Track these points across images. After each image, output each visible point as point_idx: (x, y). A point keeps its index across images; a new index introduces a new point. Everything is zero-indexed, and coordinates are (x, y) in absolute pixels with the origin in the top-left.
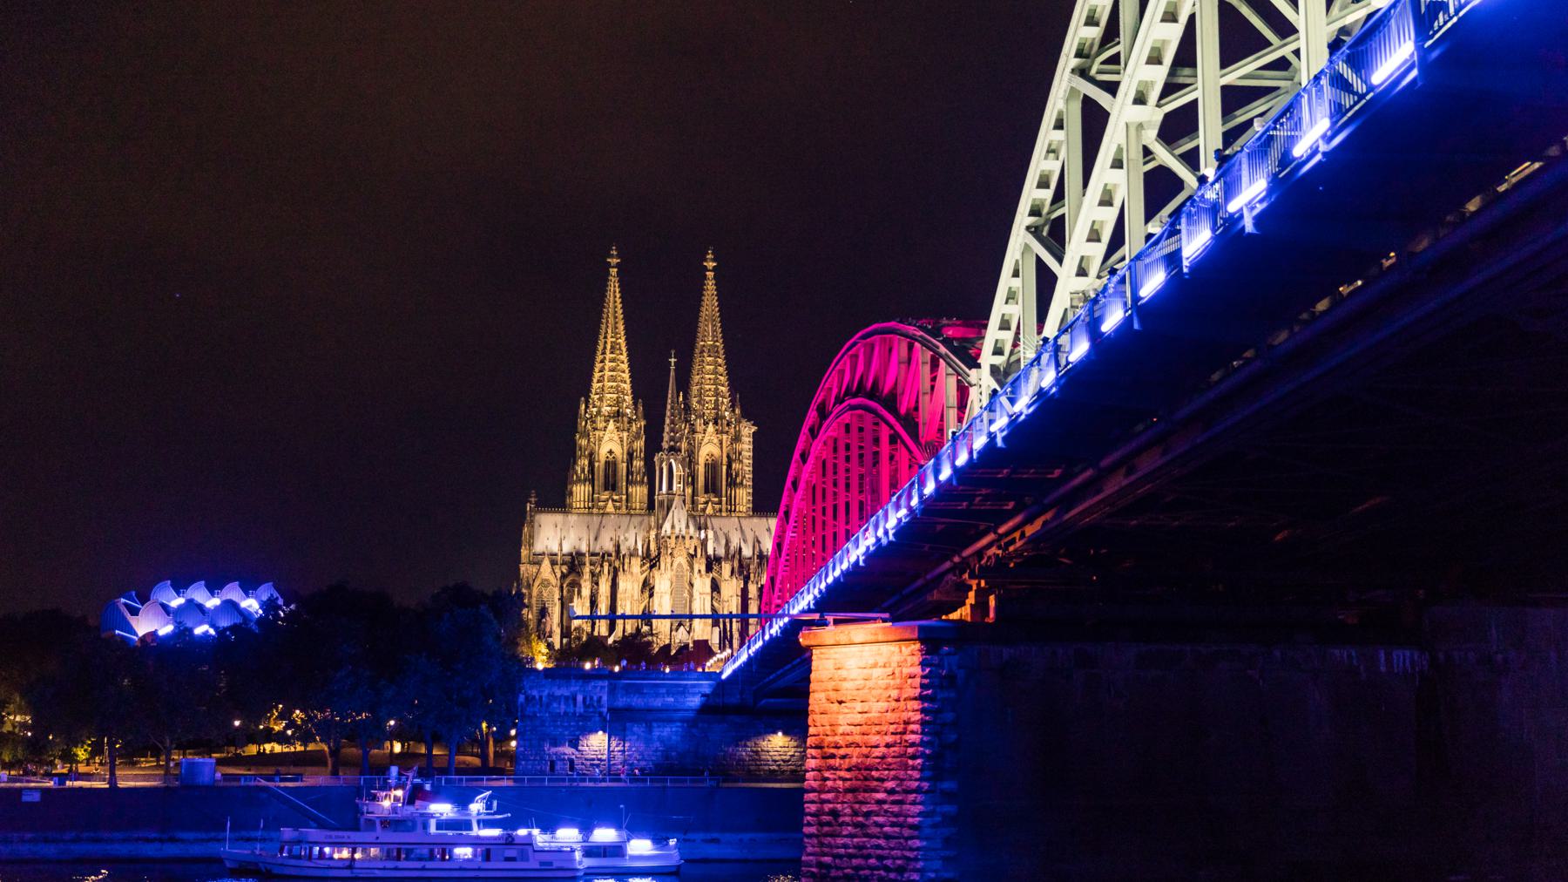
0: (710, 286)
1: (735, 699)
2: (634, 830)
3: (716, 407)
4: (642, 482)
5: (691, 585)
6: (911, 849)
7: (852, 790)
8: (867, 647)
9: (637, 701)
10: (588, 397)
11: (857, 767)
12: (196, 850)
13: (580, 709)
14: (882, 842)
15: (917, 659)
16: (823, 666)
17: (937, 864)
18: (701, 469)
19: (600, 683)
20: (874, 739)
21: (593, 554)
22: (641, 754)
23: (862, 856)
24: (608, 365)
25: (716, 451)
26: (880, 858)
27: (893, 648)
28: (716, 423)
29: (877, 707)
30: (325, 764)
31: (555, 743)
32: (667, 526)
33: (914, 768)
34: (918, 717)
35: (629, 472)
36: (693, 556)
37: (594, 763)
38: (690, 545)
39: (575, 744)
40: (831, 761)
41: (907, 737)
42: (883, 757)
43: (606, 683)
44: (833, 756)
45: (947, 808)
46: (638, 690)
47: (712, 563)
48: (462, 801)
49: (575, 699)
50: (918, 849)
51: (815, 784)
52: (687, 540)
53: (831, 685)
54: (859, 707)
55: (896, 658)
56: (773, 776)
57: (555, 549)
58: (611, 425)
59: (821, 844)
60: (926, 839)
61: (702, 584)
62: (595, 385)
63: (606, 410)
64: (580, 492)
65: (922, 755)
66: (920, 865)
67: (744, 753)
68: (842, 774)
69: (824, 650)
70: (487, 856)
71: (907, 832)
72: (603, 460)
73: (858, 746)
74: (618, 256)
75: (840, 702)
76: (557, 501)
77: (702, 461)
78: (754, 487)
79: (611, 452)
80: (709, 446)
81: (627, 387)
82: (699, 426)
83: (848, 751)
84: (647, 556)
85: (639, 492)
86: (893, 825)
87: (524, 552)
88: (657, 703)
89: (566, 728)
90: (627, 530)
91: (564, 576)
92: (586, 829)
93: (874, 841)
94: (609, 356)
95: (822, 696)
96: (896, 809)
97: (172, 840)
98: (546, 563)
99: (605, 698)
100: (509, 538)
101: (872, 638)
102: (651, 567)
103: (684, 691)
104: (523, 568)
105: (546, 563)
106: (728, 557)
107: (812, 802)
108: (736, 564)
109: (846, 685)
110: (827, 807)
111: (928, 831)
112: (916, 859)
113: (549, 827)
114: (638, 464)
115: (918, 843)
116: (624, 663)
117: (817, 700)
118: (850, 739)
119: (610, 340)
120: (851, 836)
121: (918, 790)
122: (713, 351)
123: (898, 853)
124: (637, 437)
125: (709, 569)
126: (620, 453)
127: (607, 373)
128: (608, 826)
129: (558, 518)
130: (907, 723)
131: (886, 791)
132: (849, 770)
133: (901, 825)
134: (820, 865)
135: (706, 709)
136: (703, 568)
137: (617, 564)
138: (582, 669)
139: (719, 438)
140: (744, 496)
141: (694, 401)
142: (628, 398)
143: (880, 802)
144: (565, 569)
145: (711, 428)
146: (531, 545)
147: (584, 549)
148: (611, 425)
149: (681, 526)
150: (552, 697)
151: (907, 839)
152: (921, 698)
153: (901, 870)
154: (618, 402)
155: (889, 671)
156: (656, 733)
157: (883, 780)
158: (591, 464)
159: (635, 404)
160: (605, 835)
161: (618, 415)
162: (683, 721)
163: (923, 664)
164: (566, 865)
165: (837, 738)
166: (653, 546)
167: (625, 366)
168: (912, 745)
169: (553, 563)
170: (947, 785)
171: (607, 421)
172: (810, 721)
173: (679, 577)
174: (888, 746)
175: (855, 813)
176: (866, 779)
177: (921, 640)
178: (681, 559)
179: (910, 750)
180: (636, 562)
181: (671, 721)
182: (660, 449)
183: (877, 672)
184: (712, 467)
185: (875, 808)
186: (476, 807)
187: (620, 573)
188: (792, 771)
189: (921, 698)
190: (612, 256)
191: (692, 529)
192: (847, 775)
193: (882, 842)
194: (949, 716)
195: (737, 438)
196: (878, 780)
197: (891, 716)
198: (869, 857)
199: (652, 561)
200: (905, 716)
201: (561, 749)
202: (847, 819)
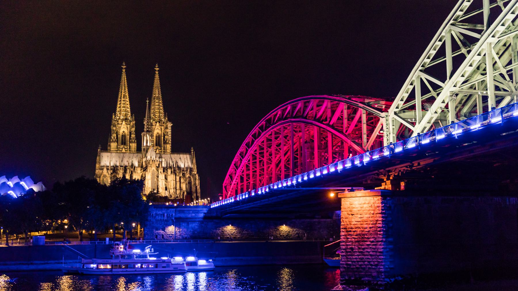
0: (157, 76)
1: (214, 215)
2: (199, 257)
3: (160, 117)
4: (134, 142)
5: (158, 177)
6: (380, 259)
7: (358, 242)
8: (362, 198)
9: (182, 215)
10: (115, 113)
11: (359, 234)
12: (41, 267)
13: (165, 218)
14: (369, 257)
15: (380, 201)
16: (345, 203)
17: (388, 263)
18: (155, 138)
19: (172, 210)
20: (365, 226)
21: (121, 166)
22: (185, 232)
23: (362, 262)
24: (122, 102)
25: (160, 132)
26: (369, 262)
27: (371, 198)
28: (159, 122)
29: (365, 216)
30: (77, 237)
31: (157, 230)
32: (149, 157)
33: (380, 234)
34: (381, 219)
35: (130, 139)
36: (158, 167)
37: (170, 236)
38: (157, 163)
39: (164, 229)
40: (350, 233)
41: (377, 225)
42: (369, 231)
43: (174, 209)
44: (351, 231)
45: (391, 246)
46: (183, 212)
47: (165, 170)
48: (143, 249)
49: (164, 215)
50: (383, 259)
51: (344, 240)
52: (156, 162)
53: (348, 210)
54: (359, 216)
55: (372, 201)
56: (228, 239)
57: (108, 164)
58: (124, 123)
59: (347, 258)
60: (385, 256)
61: (162, 177)
62: (118, 109)
63: (122, 117)
64: (113, 145)
65: (383, 231)
66: (383, 264)
67: (219, 232)
68: (354, 237)
69: (346, 199)
70: (156, 266)
71: (378, 254)
72: (121, 134)
73: (360, 228)
74: (125, 65)
75: (352, 215)
76: (106, 149)
77: (155, 135)
78: (172, 144)
79: (124, 132)
80: (157, 130)
81: (129, 110)
82: (154, 124)
83: (356, 229)
84: (142, 167)
85: (134, 146)
86: (373, 252)
87: (97, 166)
88: (190, 216)
89: (161, 224)
90: (132, 158)
91: (111, 174)
92: (184, 257)
93: (366, 257)
94: (123, 99)
95: (346, 213)
96: (374, 247)
97: (32, 264)
98: (105, 169)
99: (174, 214)
100: (92, 160)
101: (364, 195)
102: (144, 171)
103: (198, 212)
104: (97, 172)
105: (105, 169)
106: (170, 168)
107: (343, 245)
108: (173, 170)
109: (354, 209)
110: (349, 247)
111: (385, 253)
112: (382, 262)
113: (172, 256)
114: (133, 136)
115: (382, 257)
116: (178, 203)
117: (344, 214)
118: (357, 226)
119: (123, 94)
120: (358, 255)
121: (382, 241)
122: (158, 98)
123: (376, 260)
124: (133, 127)
125: (164, 171)
126: (127, 132)
127: (122, 105)
128: (192, 256)
129: (109, 154)
130: (377, 221)
131: (370, 241)
132: (356, 235)
133: (376, 252)
134: (347, 264)
135: (205, 218)
136: (162, 171)
137: (132, 170)
138: (165, 205)
139: (160, 127)
140: (169, 147)
141: (152, 116)
142: (129, 114)
143: (368, 245)
144: (112, 171)
145: (158, 124)
146: (100, 163)
147: (118, 164)
149: (154, 157)
150: (156, 214)
151: (378, 256)
152: (381, 213)
153: (376, 265)
154: (126, 115)
155: (370, 205)
156: (190, 226)
157: (369, 238)
159: (132, 116)
160: (191, 259)
161: (126, 119)
162: (199, 221)
163: (382, 203)
164: (182, 269)
165: (352, 226)
166: (144, 164)
167: (128, 103)
168: (379, 227)
169: (108, 169)
170: (390, 239)
171: (122, 121)
172: (342, 221)
173: (153, 174)
174: (370, 228)
175: (359, 248)
176: (363, 238)
177: (381, 196)
178: (154, 168)
179: (378, 229)
180: (139, 169)
181: (195, 222)
182: (143, 131)
183: (365, 206)
184: (158, 137)
185: (366, 247)
186: (147, 251)
187: (134, 174)
188: (234, 237)
189: (381, 213)
190: (123, 65)
191: (157, 158)
192: (356, 237)
193: (369, 257)
194: (390, 219)
195: (166, 128)
196: (367, 238)
197: (371, 219)
198: (365, 261)
199: (145, 169)
200: (376, 219)
201: (159, 231)
202: (357, 250)
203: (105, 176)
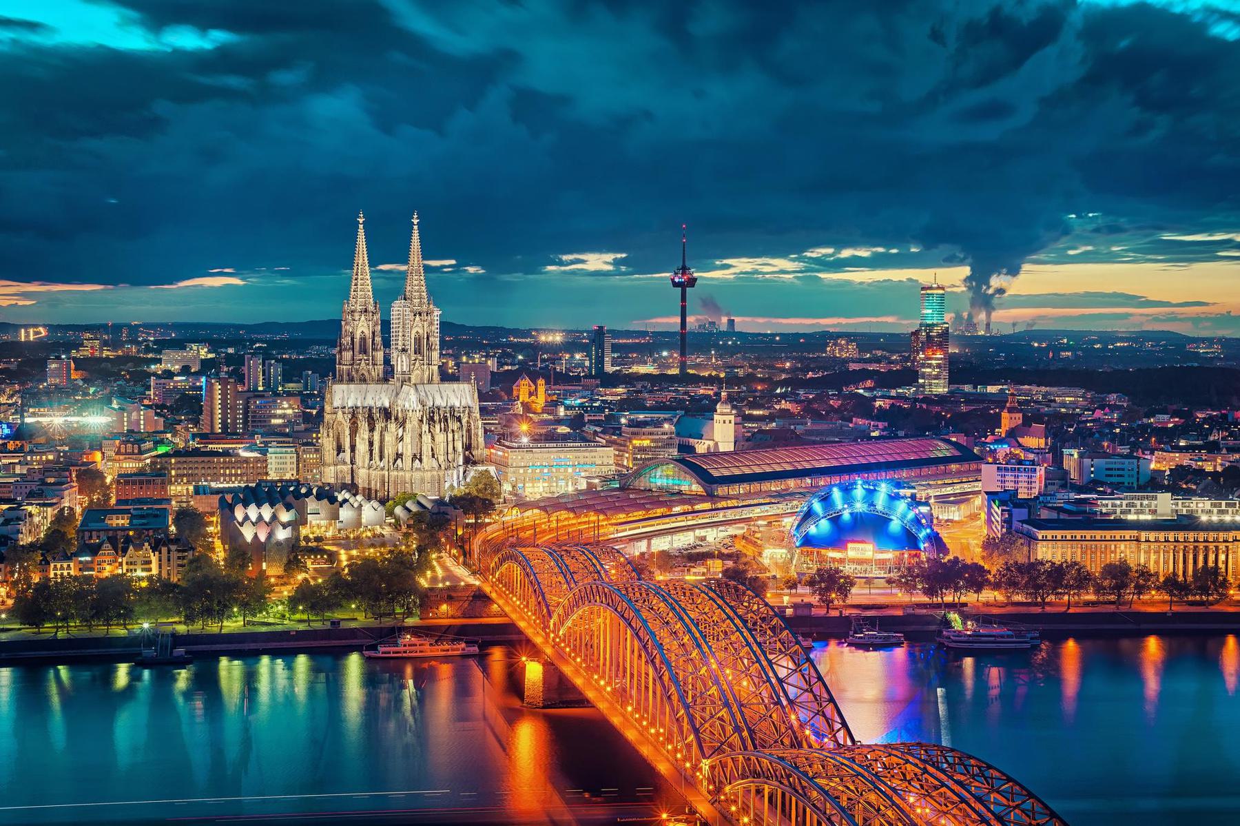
25: (421, 331)
35: (373, 343)
38: (419, 415)
58: (363, 318)
61: (427, 438)
63: (359, 308)
85: (380, 356)
87: (328, 408)
98: (340, 413)
104: (327, 417)
105: (340, 413)
126: (368, 333)
129: (344, 387)
148: (363, 318)
158: (352, 339)
178: (416, 423)
184: (418, 340)
203: (340, 423)
